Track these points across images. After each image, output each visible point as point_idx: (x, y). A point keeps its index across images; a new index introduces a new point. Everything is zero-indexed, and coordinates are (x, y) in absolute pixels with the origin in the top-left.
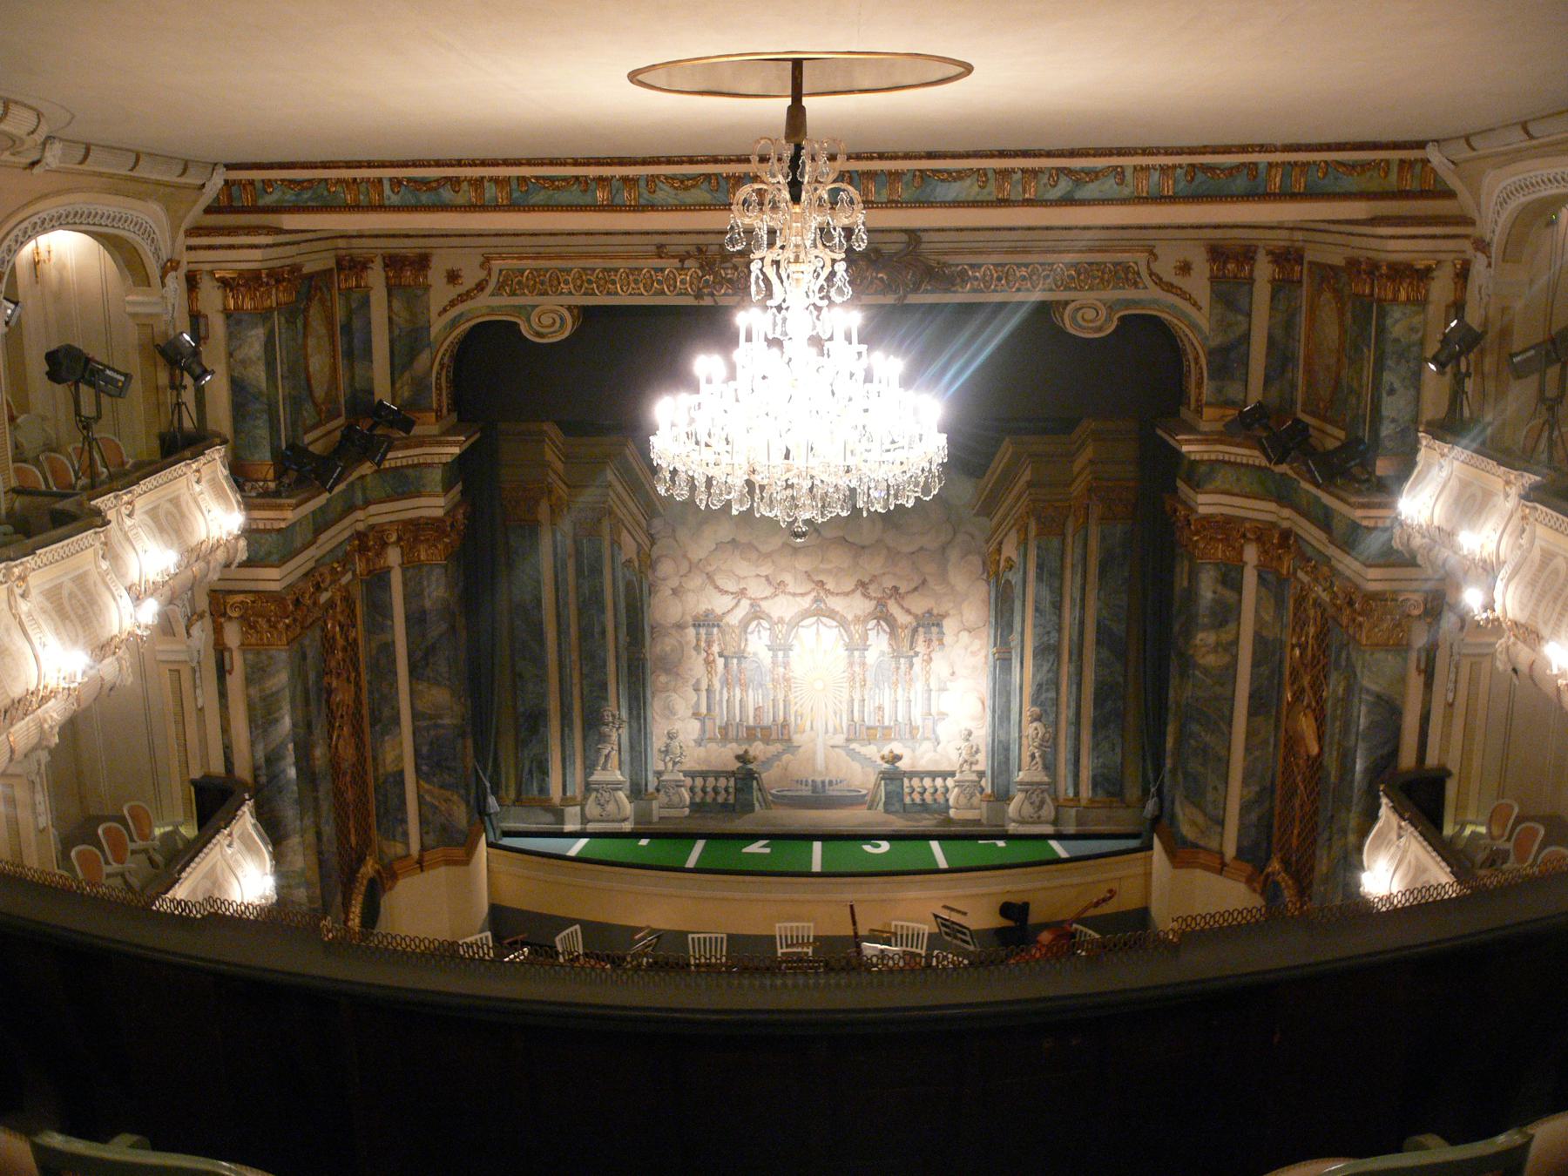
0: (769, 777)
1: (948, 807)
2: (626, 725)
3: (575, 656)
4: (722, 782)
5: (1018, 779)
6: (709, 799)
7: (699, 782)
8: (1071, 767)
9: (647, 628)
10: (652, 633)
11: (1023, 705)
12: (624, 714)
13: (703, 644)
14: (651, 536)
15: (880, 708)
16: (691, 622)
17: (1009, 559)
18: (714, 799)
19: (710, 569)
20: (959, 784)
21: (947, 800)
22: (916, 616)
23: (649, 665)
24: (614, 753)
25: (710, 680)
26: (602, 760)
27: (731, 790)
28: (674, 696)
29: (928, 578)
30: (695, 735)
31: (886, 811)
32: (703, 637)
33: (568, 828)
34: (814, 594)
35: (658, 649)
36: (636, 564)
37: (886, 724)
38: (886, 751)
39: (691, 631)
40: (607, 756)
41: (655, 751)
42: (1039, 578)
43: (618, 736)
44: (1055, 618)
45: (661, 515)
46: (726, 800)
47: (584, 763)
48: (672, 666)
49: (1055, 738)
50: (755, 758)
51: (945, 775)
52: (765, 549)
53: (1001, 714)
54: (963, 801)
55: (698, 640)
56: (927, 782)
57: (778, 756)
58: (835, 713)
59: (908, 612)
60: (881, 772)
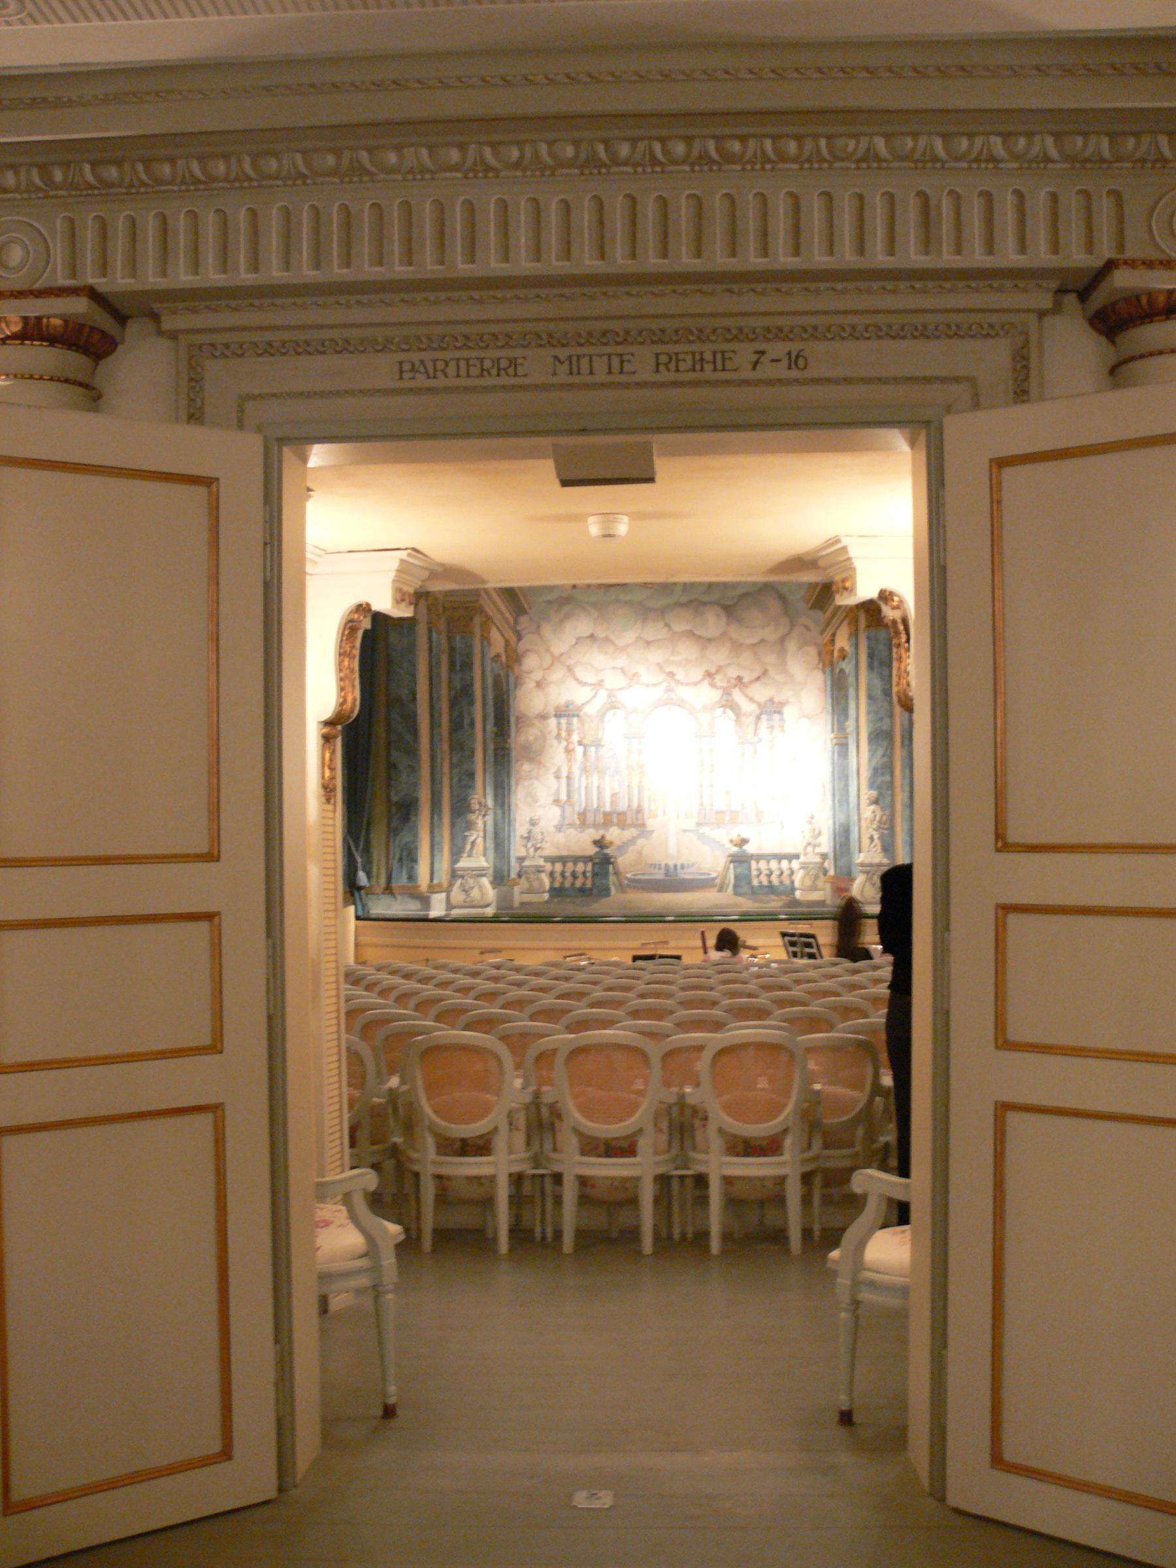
0: (624, 861)
1: (793, 889)
2: (491, 813)
3: (446, 747)
4: (580, 867)
5: (859, 861)
6: (567, 884)
7: (558, 867)
8: (907, 849)
9: (512, 719)
10: (517, 725)
11: (862, 790)
12: (490, 802)
13: (564, 734)
16: (553, 712)
17: (842, 650)
18: (573, 884)
19: (570, 662)
20: (804, 866)
21: (792, 882)
22: (759, 704)
23: (513, 754)
24: (480, 841)
25: (570, 768)
26: (468, 847)
27: (588, 875)
29: (769, 668)
31: (736, 893)
32: (564, 726)
33: (433, 914)
35: (522, 739)
36: (504, 658)
39: (553, 722)
40: (473, 843)
41: (518, 838)
42: (871, 667)
43: (482, 824)
44: (886, 705)
45: (525, 612)
46: (584, 884)
47: (451, 849)
48: (533, 755)
49: (892, 819)
50: (611, 843)
51: (791, 857)
52: (620, 642)
53: (840, 794)
54: (808, 883)
55: (559, 729)
56: (774, 864)
57: (632, 841)
59: (751, 700)
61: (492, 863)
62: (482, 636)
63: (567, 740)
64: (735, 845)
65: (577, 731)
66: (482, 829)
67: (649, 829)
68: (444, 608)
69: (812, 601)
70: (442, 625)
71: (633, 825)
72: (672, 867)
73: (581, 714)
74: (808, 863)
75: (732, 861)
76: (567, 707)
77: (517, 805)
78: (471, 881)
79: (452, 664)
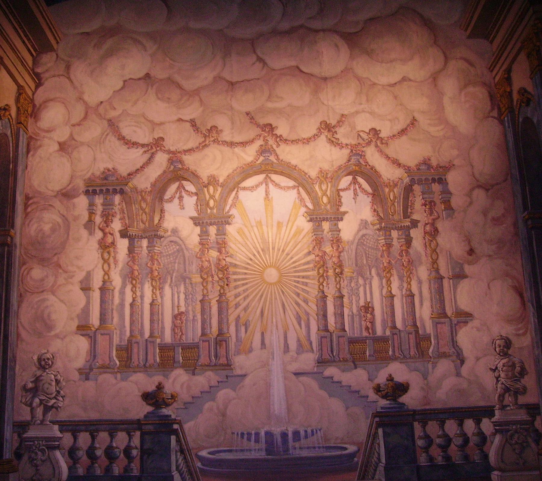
1: (489, 469)
4: (121, 439)
9: (20, 199)
10: (26, 206)
13: (98, 219)
14: (38, 75)
15: (368, 308)
16: (82, 187)
18: (108, 470)
21: (486, 457)
25: (106, 273)
28: (52, 299)
30: (80, 362)
32: (99, 209)
34: (259, 142)
35: (33, 229)
37: (379, 332)
38: (381, 378)
46: (127, 469)
50: (173, 397)
52: (189, 85)
56: (451, 427)
58: (299, 319)
60: (376, 415)
63: (102, 230)
64: (385, 397)
65: (118, 216)
67: (238, 372)
69: (470, 29)
71: (209, 366)
72: (279, 439)
73: (127, 189)
74: (508, 423)
75: (379, 425)
76: (106, 179)
77: (18, 335)
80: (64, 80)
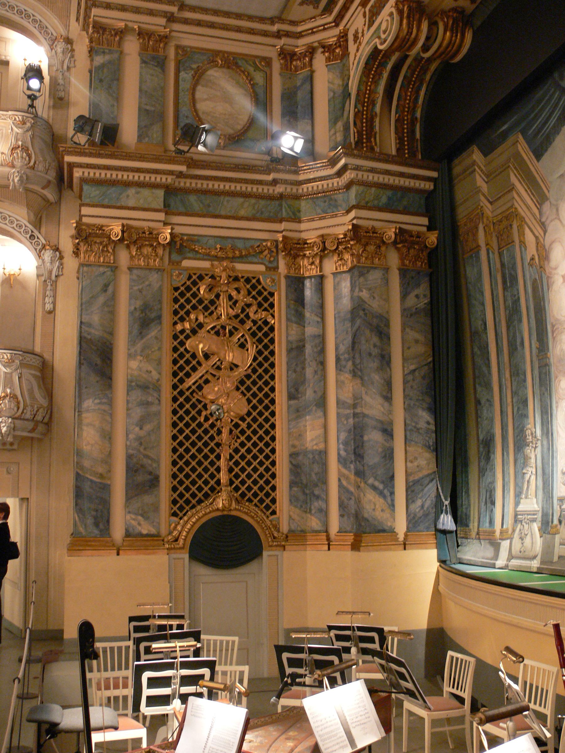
12: (539, 432)
23: (553, 369)
24: (533, 477)
40: (528, 482)
61: (540, 506)
62: (520, 242)
66: (534, 466)
68: (494, 224)
70: (495, 244)
77: (558, 432)
78: (526, 526)
79: (504, 282)
80: (557, 222)
